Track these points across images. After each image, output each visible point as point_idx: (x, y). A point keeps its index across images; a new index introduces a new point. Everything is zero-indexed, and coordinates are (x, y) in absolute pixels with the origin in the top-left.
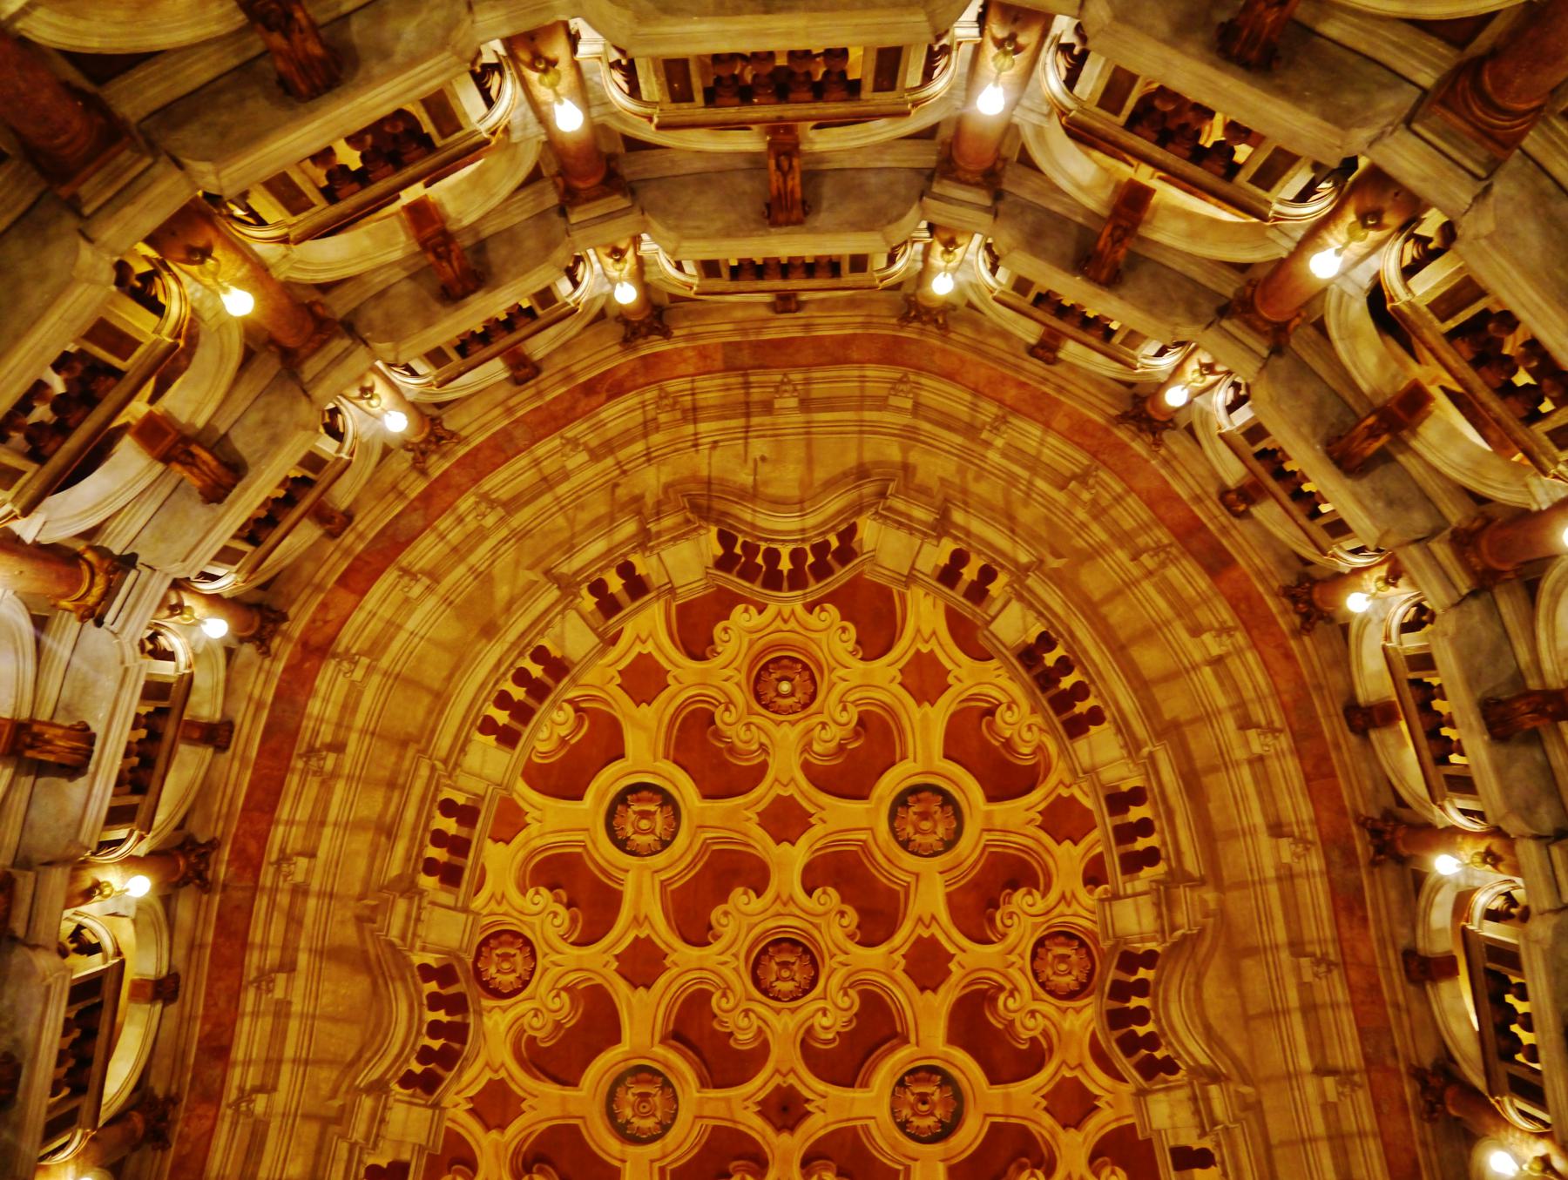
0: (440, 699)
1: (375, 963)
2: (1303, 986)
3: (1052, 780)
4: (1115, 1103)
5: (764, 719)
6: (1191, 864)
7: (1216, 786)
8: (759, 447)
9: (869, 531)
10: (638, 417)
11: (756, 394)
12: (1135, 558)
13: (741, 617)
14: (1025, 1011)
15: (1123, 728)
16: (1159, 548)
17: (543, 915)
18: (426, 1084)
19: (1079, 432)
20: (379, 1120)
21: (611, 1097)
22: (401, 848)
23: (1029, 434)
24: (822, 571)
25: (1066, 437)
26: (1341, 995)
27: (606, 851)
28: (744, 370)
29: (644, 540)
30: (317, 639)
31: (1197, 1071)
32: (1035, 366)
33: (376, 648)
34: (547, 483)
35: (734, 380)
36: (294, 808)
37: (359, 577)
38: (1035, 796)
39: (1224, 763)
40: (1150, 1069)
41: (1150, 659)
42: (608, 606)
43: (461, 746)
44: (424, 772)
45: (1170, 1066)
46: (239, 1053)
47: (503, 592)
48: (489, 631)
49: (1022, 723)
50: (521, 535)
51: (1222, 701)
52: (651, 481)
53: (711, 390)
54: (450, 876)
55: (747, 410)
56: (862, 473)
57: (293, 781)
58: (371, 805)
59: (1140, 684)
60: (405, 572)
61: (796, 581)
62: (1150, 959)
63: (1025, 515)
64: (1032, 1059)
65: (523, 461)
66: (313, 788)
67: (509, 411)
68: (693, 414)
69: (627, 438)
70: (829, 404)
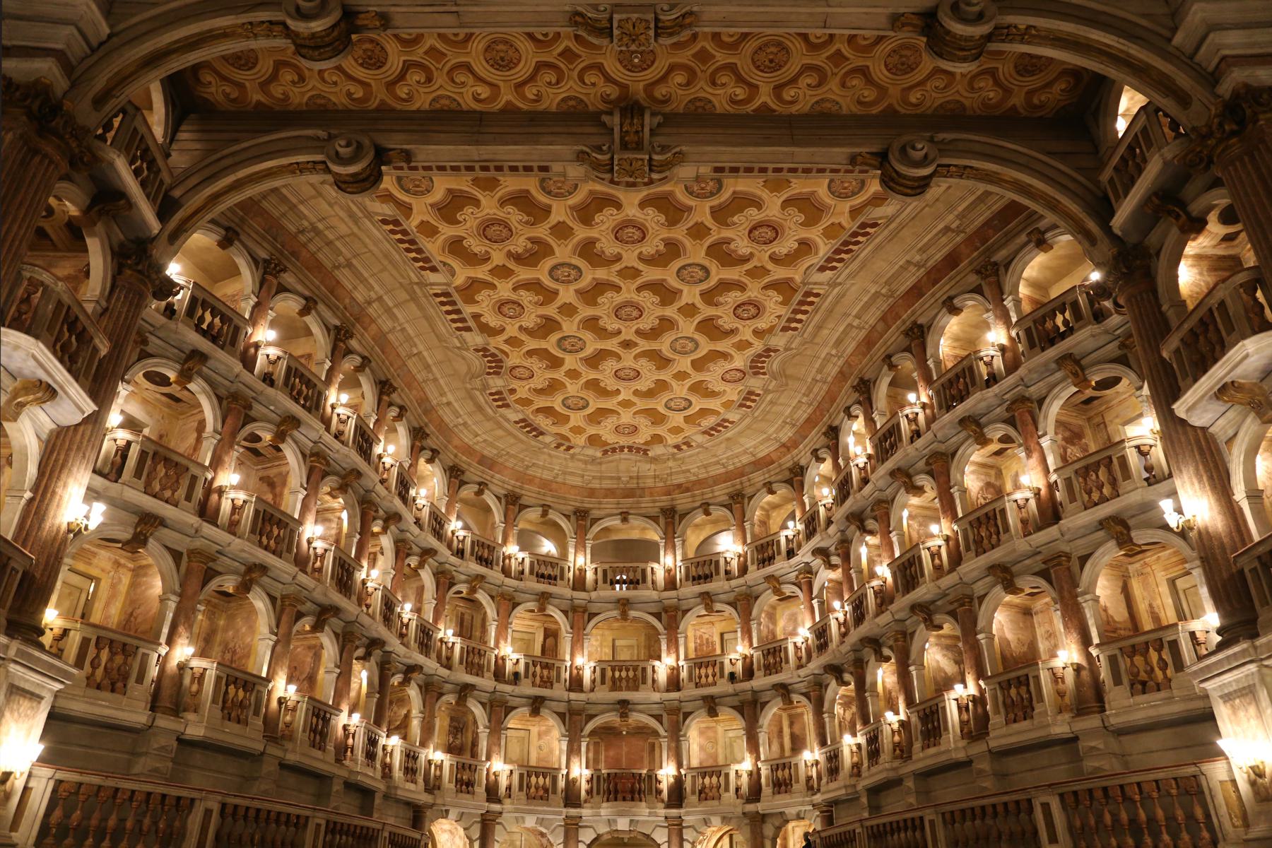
0: (748, 427)
1: (782, 375)
2: (430, 371)
4: (497, 343)
6: (478, 393)
7: (470, 406)
9: (599, 454)
14: (535, 364)
15: (508, 420)
17: (718, 386)
18: (768, 350)
19: (531, 480)
20: (790, 341)
21: (696, 348)
22: (769, 398)
23: (547, 475)
24: (614, 450)
26: (418, 376)
27: (693, 399)
28: (638, 488)
29: (673, 454)
31: (467, 349)
32: (549, 500)
33: (768, 439)
34: (705, 467)
36: (803, 414)
39: (470, 414)
40: (485, 350)
41: (500, 432)
42: (688, 444)
43: (742, 419)
45: (477, 350)
46: (836, 369)
47: (723, 445)
48: (728, 439)
49: (542, 422)
50: (715, 456)
52: (671, 464)
53: (650, 483)
54: (751, 393)
55: (638, 478)
57: (801, 421)
58: (775, 409)
59: (501, 427)
61: (622, 449)
62: (489, 374)
63: (546, 457)
64: (530, 353)
65: (712, 474)
66: (796, 416)
67: (712, 492)
69: (677, 473)
70: (612, 478)
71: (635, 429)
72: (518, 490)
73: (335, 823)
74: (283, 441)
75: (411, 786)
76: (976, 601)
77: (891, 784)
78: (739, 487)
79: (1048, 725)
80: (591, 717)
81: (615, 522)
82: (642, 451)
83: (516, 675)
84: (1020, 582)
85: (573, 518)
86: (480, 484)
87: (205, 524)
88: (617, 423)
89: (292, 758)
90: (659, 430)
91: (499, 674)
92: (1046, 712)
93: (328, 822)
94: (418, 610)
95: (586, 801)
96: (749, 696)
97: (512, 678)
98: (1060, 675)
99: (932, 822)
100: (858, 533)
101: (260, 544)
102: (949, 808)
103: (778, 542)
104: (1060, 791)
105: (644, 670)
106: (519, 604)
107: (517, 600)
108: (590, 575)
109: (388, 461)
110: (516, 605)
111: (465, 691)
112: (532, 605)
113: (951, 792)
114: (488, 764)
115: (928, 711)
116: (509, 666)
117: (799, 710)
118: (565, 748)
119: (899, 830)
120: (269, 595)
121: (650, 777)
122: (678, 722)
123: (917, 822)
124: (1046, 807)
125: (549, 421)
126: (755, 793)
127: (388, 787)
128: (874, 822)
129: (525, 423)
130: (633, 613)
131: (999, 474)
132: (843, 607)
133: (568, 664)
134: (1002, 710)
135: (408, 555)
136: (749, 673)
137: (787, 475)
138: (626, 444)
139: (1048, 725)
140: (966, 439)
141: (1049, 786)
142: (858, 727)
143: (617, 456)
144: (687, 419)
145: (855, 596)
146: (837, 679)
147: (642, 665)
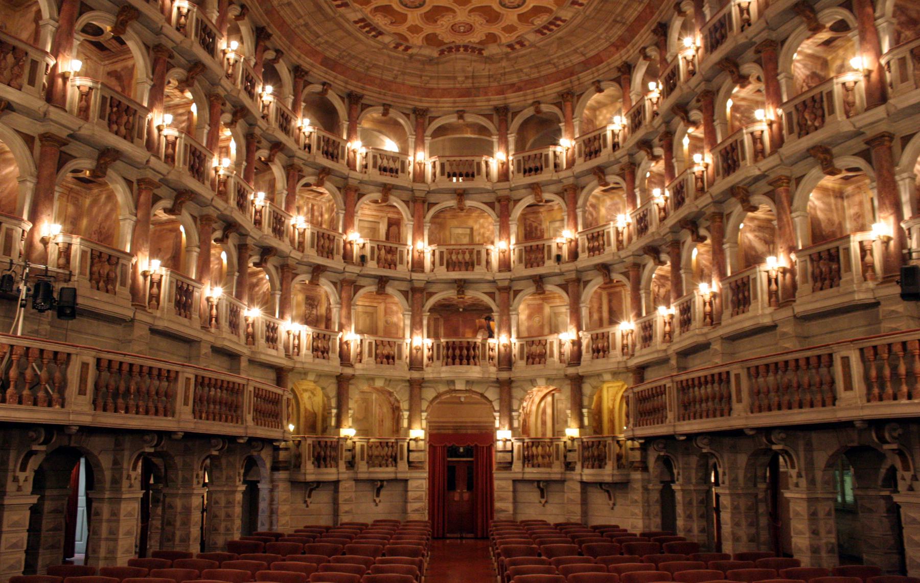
3: (369, 9)
5: (468, 21)
8: (470, 69)
9: (435, 54)
10: (507, 77)
11: (470, 81)
12: (349, 54)
13: (477, 41)
15: (347, 21)
16: (343, 58)
23: (388, 76)
25: (376, 78)
28: (474, 88)
29: (507, 54)
30: (613, 49)
32: (389, 100)
34: (537, 66)
35: (477, 85)
37: (597, 60)
38: (374, 6)
41: (340, 33)
43: (574, 18)
44: (588, 13)
48: (560, 38)
49: (380, 21)
51: (315, 28)
52: (504, 63)
53: (484, 82)
55: (473, 77)
56: (438, 64)
57: (631, 19)
59: (341, 27)
60: (584, 55)
61: (458, 48)
65: (543, 73)
67: (544, 91)
68: (489, 77)
71: (470, 29)
72: (358, 90)
73: (203, 378)
74: (124, 32)
75: (273, 352)
76: (793, 182)
77: (701, 348)
78: (569, 85)
79: (854, 292)
80: (431, 294)
81: (453, 119)
82: (477, 50)
83: (363, 258)
84: (839, 163)
85: (412, 116)
86: (324, 84)
87: (52, 109)
88: (452, 22)
89: (161, 324)
90: (496, 29)
91: (347, 257)
92: (852, 280)
93: (196, 376)
94: (271, 198)
95: (427, 366)
96: (573, 276)
97: (359, 259)
98: (868, 247)
99: (737, 376)
100: (682, 124)
101: (111, 130)
102: (756, 363)
103: (605, 136)
104: (861, 346)
105: (479, 252)
106: (364, 195)
107: (362, 191)
108: (429, 170)
109: (231, 56)
110: (361, 196)
111: (317, 271)
112: (377, 196)
113: (756, 351)
114: (340, 335)
115: (739, 282)
116: (356, 250)
117: (618, 289)
118: (408, 322)
119: (706, 382)
120: (125, 179)
121: (484, 345)
122: (509, 298)
123: (724, 377)
124: (846, 361)
125: (387, 21)
126: (576, 358)
127: (253, 352)
128: (684, 377)
129: (364, 23)
130: (468, 203)
131: (825, 64)
132: (663, 193)
133: (410, 249)
134: (810, 279)
135: (258, 148)
136: (574, 255)
137: (615, 75)
138: (461, 43)
139: (854, 292)
140: (798, 26)
141: (851, 341)
142: (672, 300)
143: (453, 56)
144: (521, 17)
145: (676, 182)
146: (655, 259)
147: (477, 248)
